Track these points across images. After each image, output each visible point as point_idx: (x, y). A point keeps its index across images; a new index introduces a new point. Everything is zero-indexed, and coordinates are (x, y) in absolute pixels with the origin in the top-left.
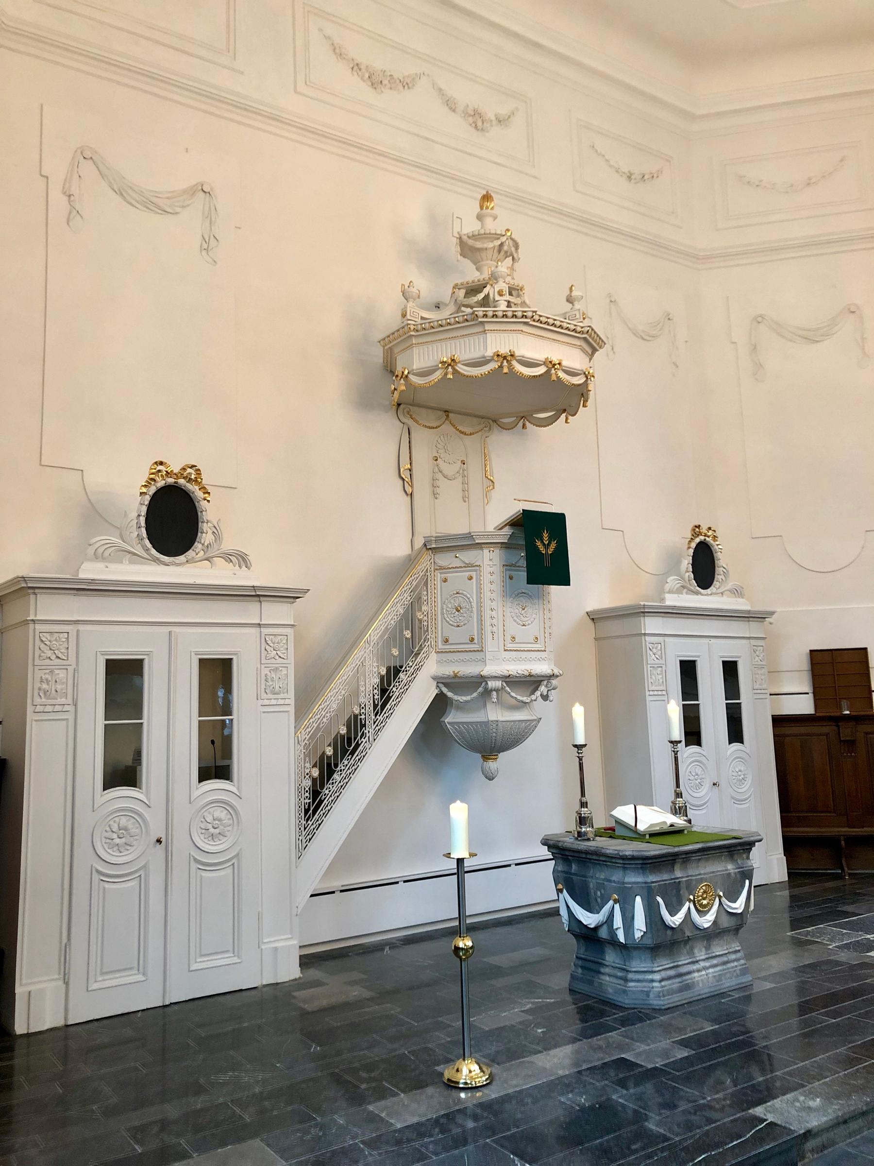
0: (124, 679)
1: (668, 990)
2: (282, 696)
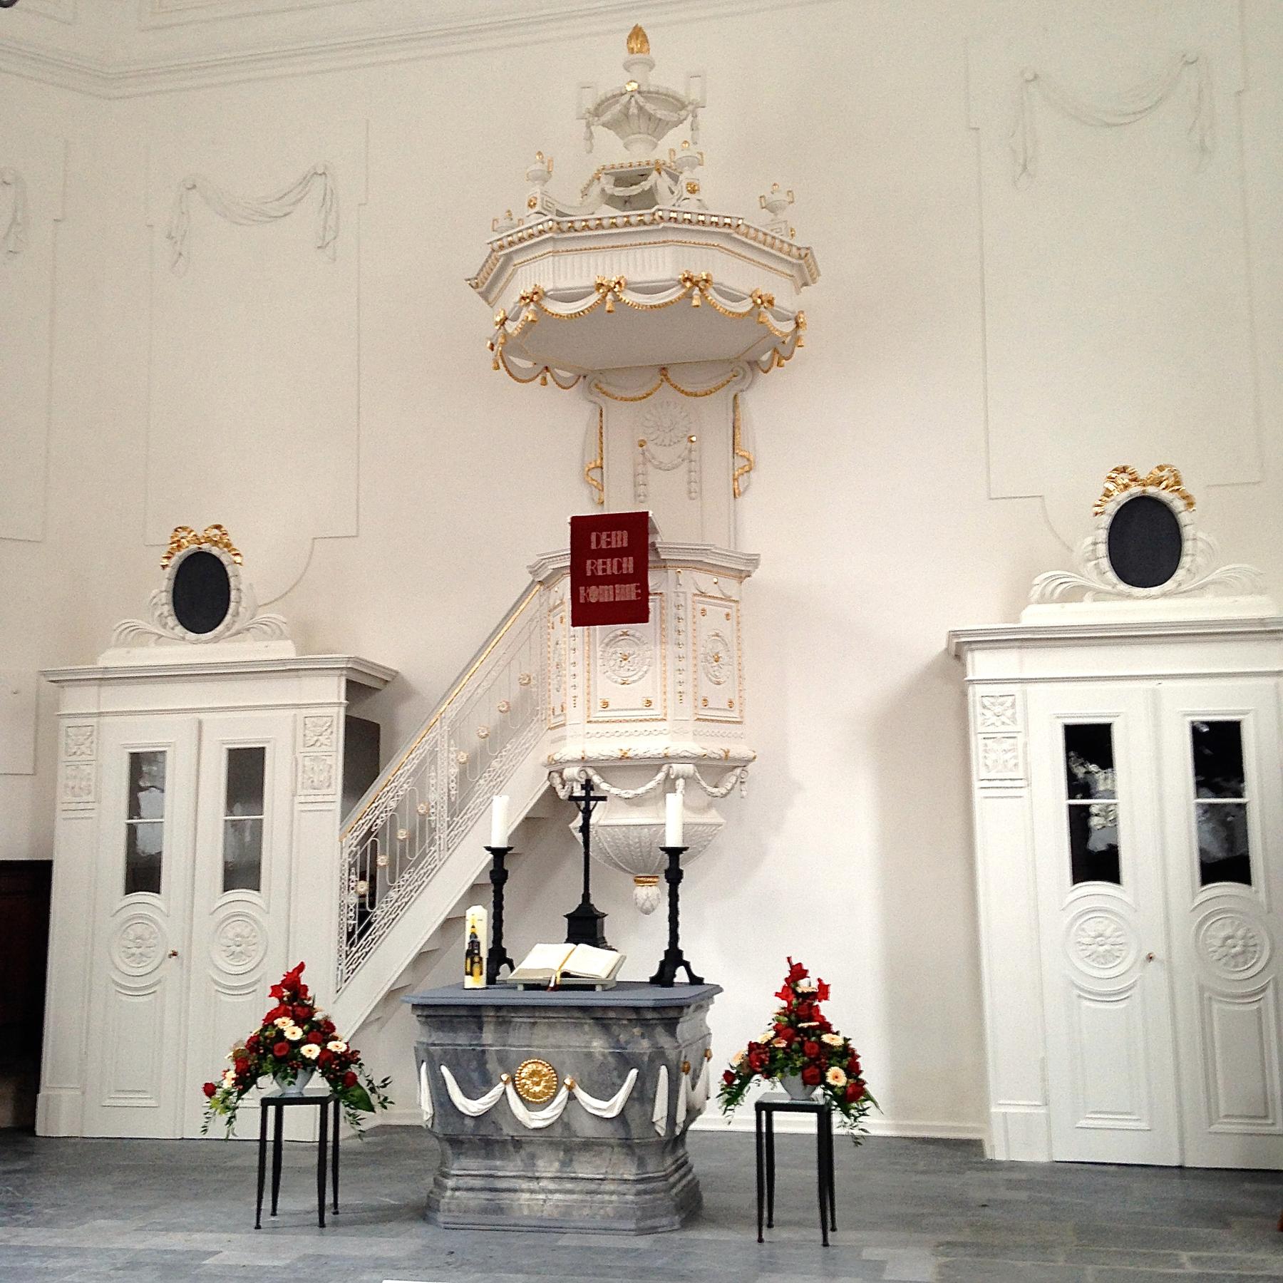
2: (325, 791)
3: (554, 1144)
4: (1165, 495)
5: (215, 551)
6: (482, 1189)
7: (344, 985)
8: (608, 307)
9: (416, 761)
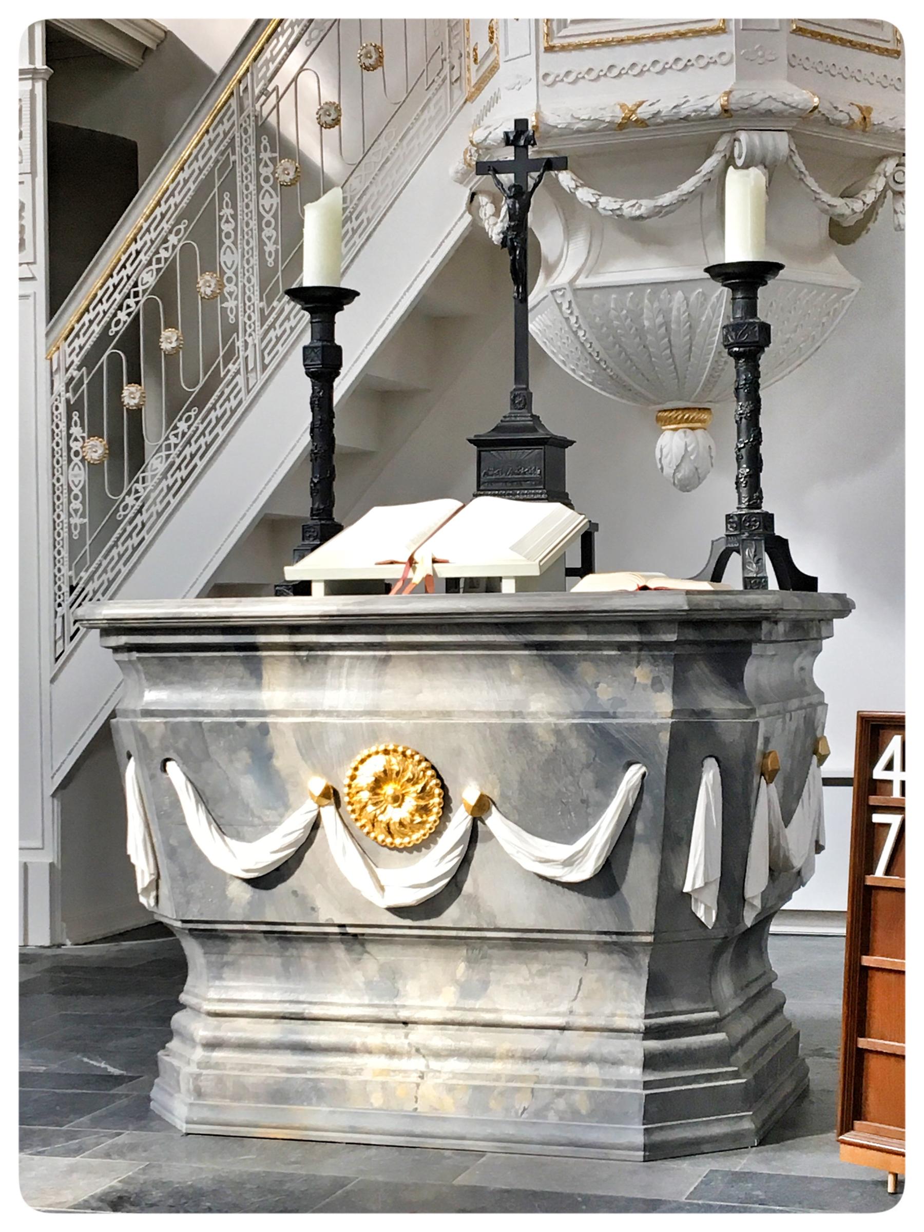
1: (220, 1080)
7: (69, 647)
9: (191, 186)
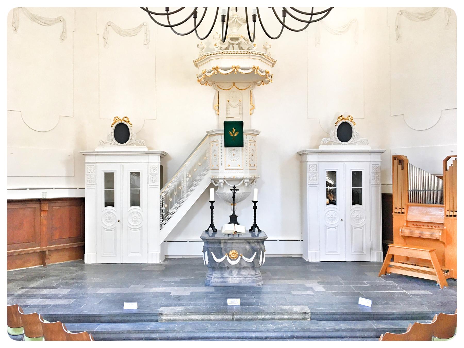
0: (109, 178)
3: (237, 268)
4: (350, 122)
5: (126, 123)
6: (220, 278)
8: (236, 73)
